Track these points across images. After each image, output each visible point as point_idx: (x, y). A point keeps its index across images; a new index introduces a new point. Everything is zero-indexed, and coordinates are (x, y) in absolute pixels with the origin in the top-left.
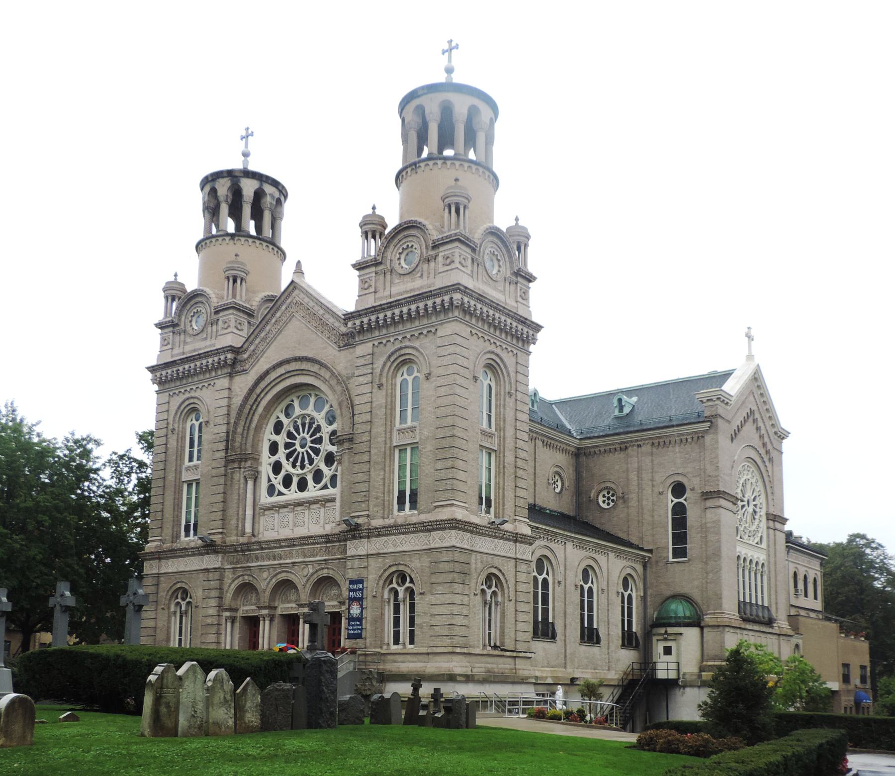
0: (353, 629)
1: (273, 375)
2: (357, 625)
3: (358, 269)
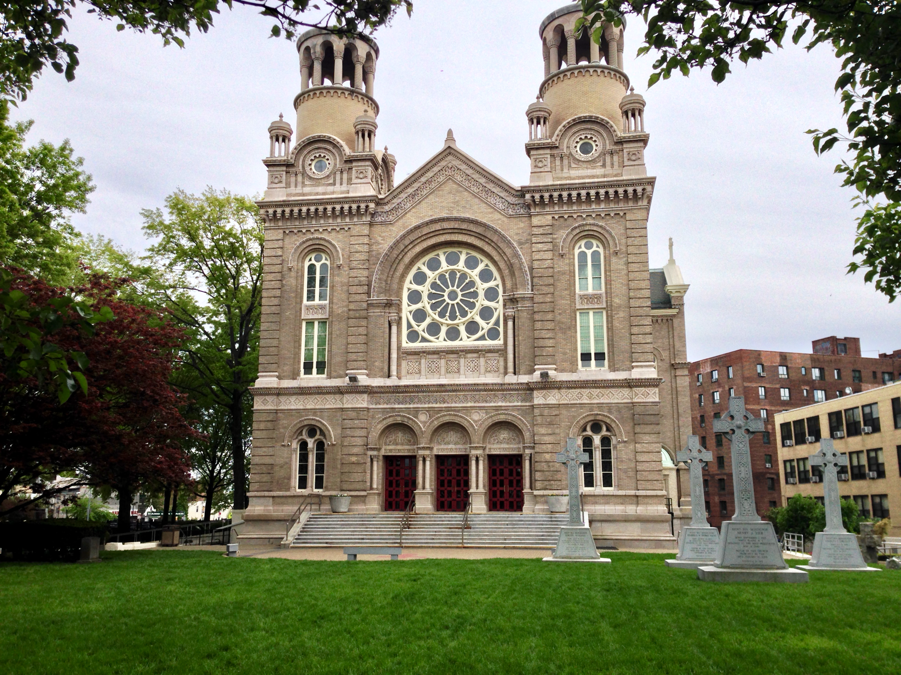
3: (268, 166)
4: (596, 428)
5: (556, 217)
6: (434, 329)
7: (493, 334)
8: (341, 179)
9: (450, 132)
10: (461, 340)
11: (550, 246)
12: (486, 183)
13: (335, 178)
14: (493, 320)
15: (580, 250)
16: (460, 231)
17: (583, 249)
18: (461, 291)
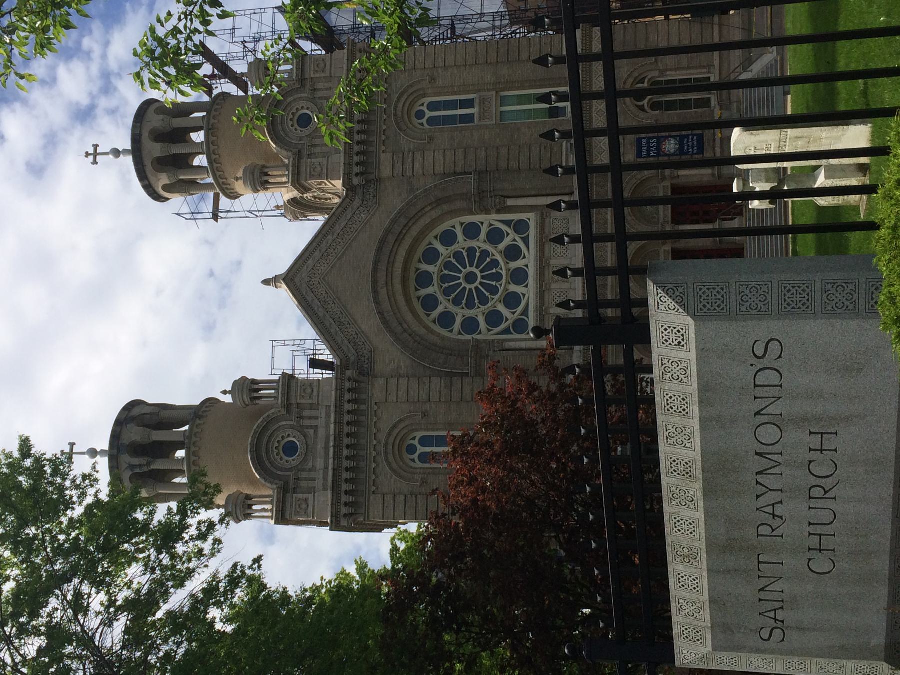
0: (693, 148)
1: (386, 305)
2: (688, 142)
5: (384, 148)
6: (512, 301)
7: (520, 227)
8: (310, 418)
9: (266, 282)
10: (527, 266)
11: (418, 156)
12: (333, 234)
13: (308, 427)
14: (504, 228)
15: (425, 124)
16: (391, 263)
17: (424, 121)
18: (465, 268)
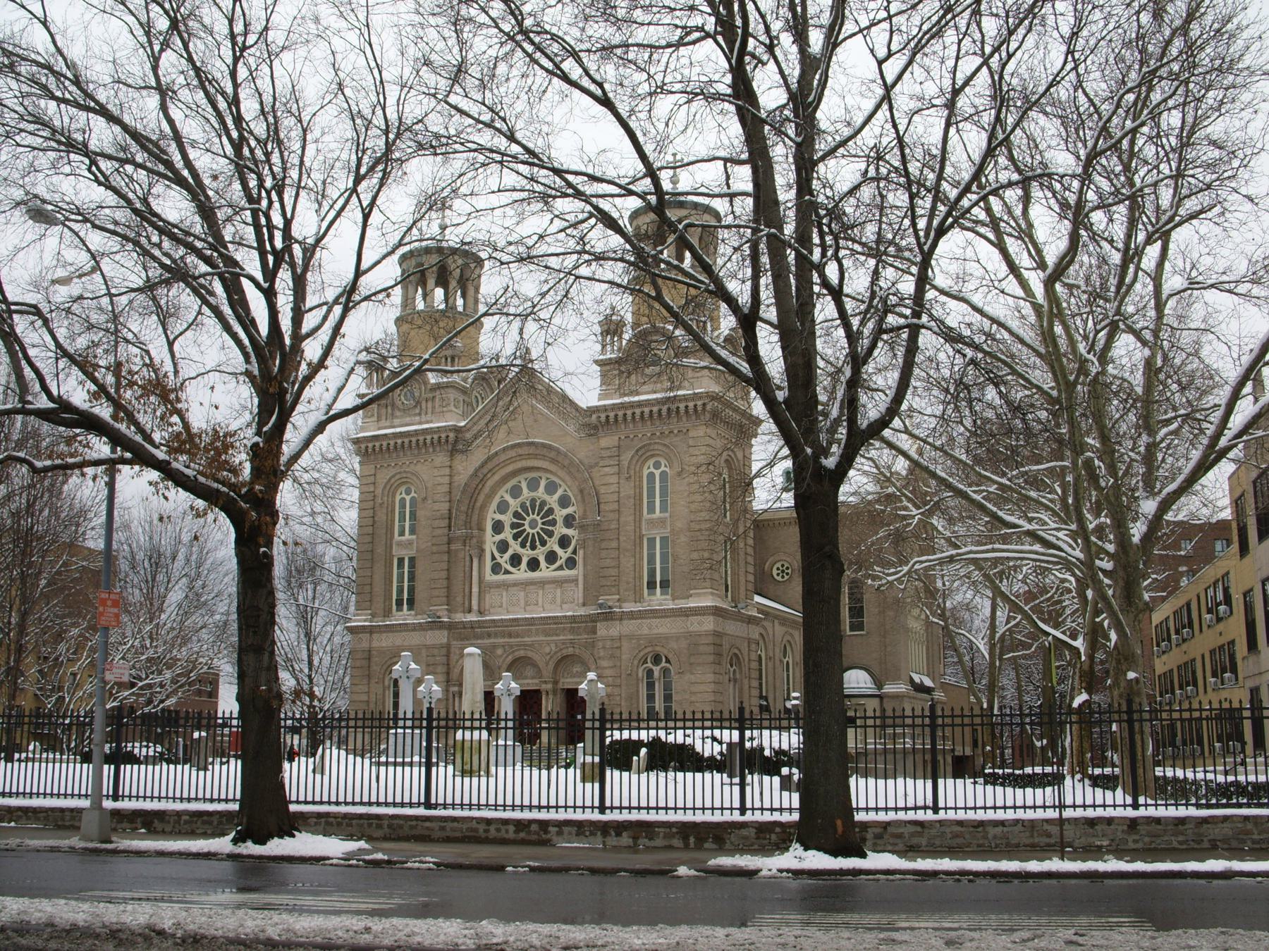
1: (503, 457)
4: (657, 659)
6: (516, 560)
7: (571, 563)
14: (570, 549)
16: (536, 456)
17: (652, 469)
